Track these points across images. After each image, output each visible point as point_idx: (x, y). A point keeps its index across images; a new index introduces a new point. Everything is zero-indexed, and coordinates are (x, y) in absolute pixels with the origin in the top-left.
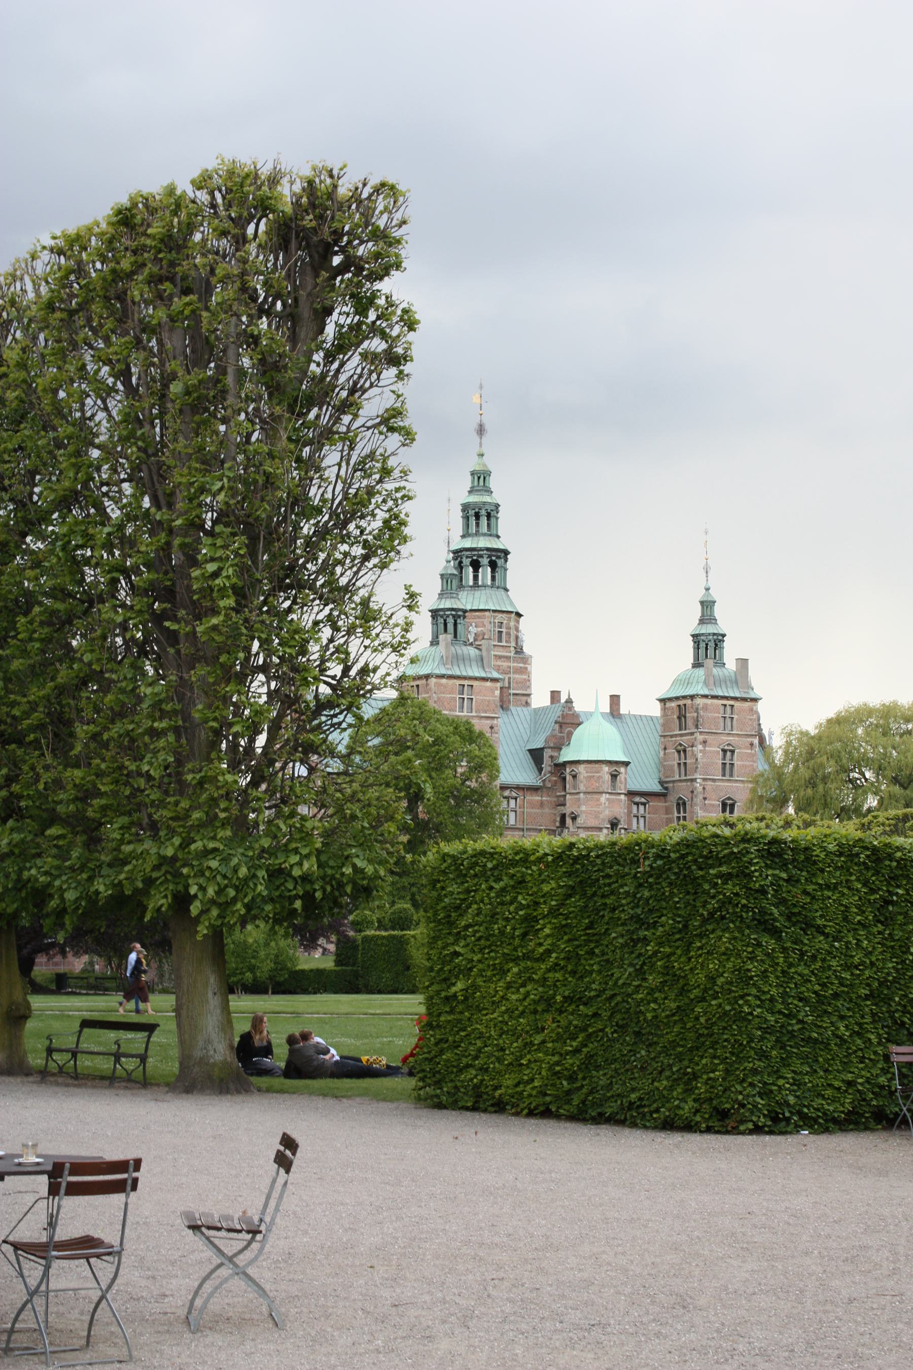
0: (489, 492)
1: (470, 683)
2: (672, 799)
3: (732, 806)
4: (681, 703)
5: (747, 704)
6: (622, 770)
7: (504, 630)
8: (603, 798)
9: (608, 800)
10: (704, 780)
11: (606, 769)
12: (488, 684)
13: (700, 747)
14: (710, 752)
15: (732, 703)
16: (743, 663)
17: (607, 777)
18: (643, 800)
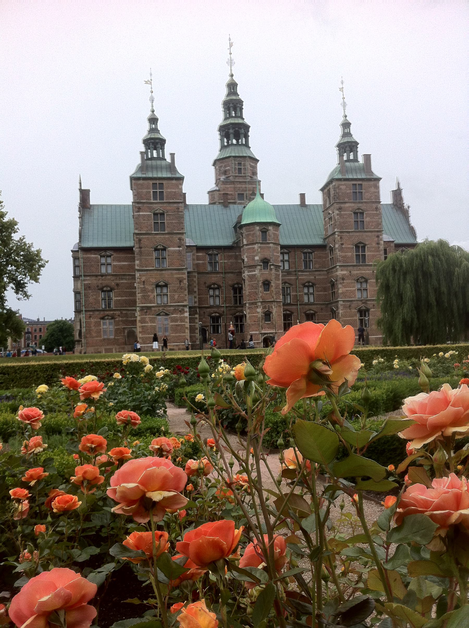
0: (236, 94)
1: (161, 182)
2: (328, 248)
3: (364, 247)
4: (328, 188)
5: (372, 183)
6: (270, 228)
7: (242, 167)
8: (256, 246)
9: (260, 247)
10: (341, 232)
11: (258, 228)
12: (174, 182)
13: (337, 212)
14: (345, 214)
15: (360, 182)
16: (367, 158)
17: (259, 233)
18: (309, 250)
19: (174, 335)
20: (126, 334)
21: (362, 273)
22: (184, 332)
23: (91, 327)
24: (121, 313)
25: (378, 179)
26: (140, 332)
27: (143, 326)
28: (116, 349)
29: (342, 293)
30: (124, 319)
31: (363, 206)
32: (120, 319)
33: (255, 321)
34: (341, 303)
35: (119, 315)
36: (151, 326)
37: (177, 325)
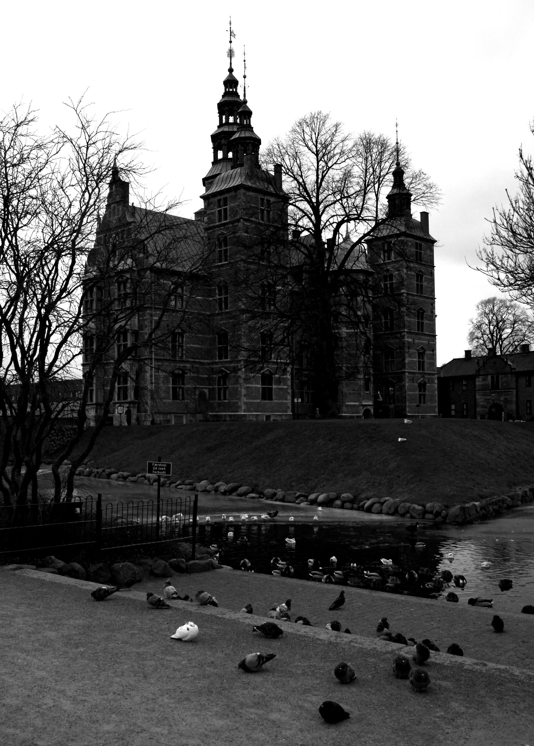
16: (425, 215)
19: (276, 401)
20: (197, 397)
21: (421, 343)
22: (286, 399)
23: (159, 384)
24: (193, 367)
25: (434, 241)
26: (245, 396)
27: (247, 387)
28: (186, 418)
29: (408, 363)
30: (195, 375)
31: (423, 269)
32: (192, 375)
33: (353, 390)
34: (407, 374)
35: (190, 370)
36: (255, 388)
37: (280, 389)
